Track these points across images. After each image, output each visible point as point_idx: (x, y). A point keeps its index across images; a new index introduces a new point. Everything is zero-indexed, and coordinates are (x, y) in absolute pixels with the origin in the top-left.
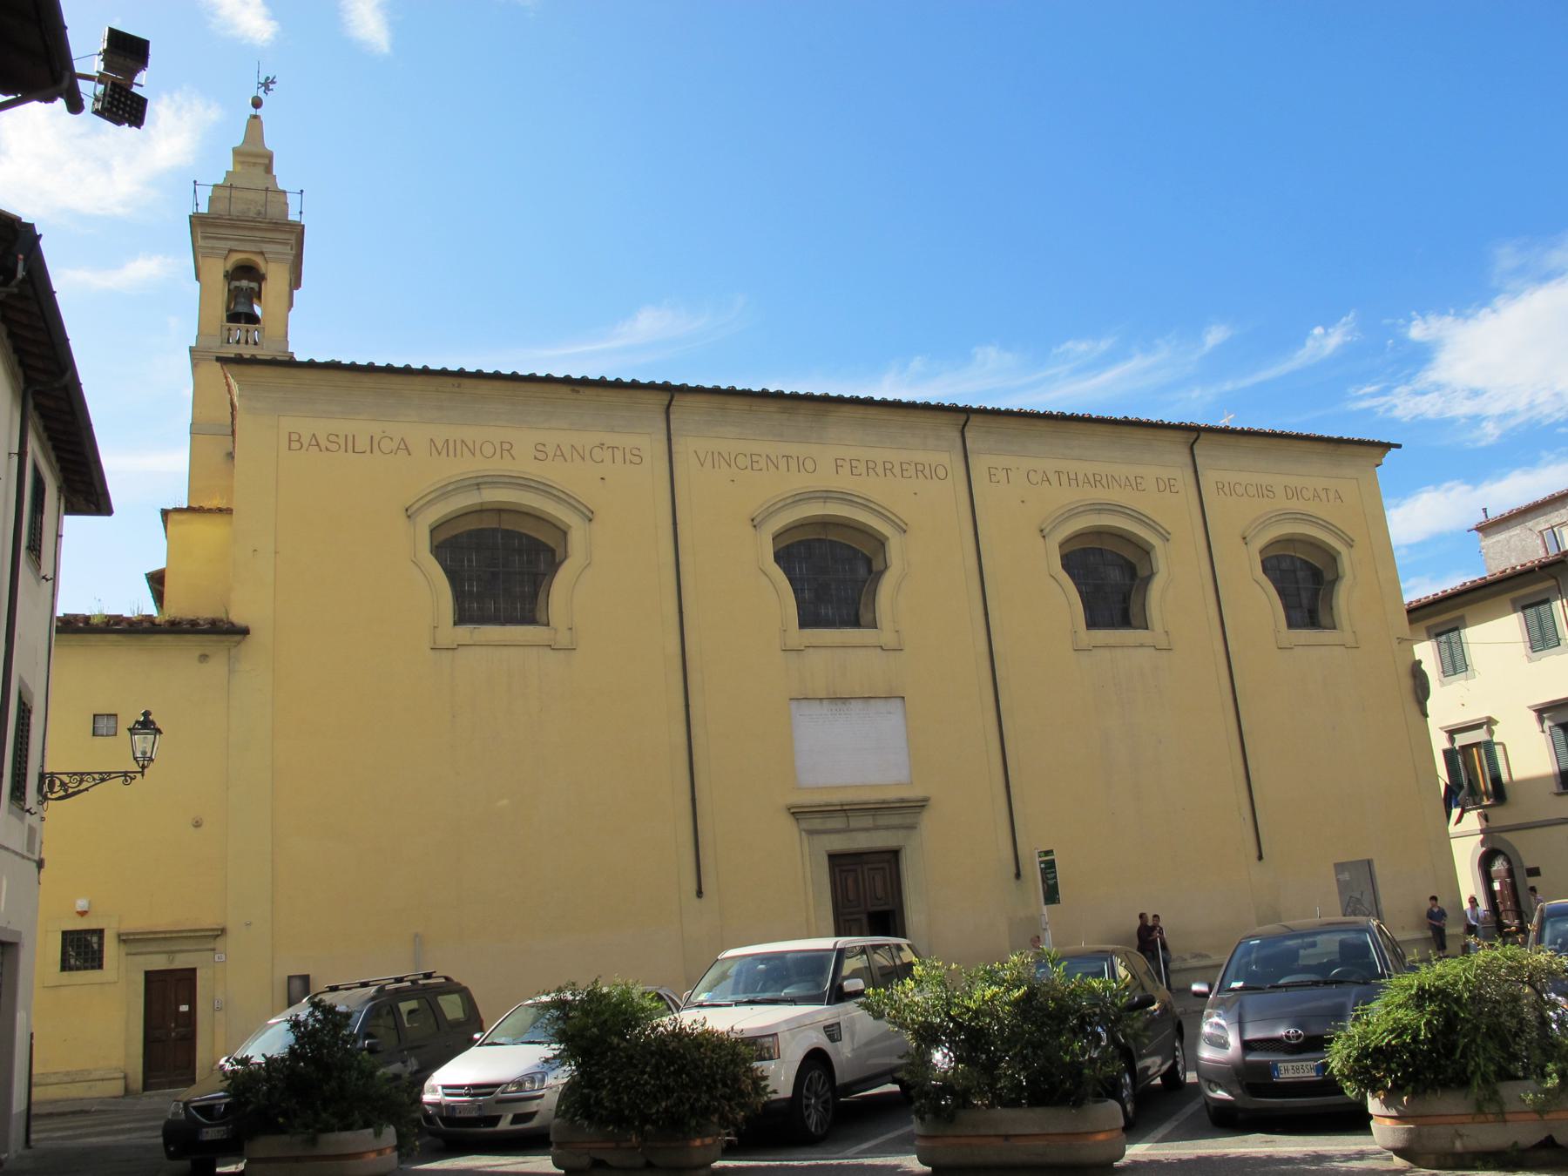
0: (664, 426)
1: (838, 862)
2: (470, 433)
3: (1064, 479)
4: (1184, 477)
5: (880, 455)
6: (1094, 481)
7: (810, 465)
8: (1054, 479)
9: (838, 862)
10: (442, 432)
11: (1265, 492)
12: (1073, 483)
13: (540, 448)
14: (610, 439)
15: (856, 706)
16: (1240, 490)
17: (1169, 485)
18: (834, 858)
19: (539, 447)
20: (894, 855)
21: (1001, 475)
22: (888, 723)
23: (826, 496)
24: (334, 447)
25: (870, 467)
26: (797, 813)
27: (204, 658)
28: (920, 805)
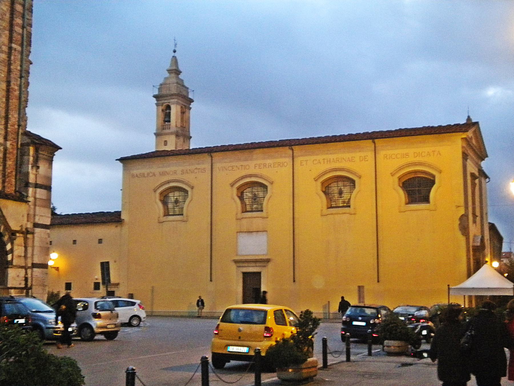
0: (210, 161)
1: (245, 275)
2: (167, 169)
3: (326, 161)
4: (370, 155)
5: (269, 161)
6: (338, 160)
7: (247, 167)
8: (322, 161)
9: (245, 275)
10: (161, 170)
11: (405, 156)
12: (329, 162)
13: (182, 171)
14: (198, 166)
15: (254, 234)
16: (399, 156)
17: (365, 159)
18: (244, 274)
19: (182, 171)
20: (259, 274)
21: (304, 163)
22: (262, 238)
23: (250, 176)
24: (140, 176)
25: (265, 165)
26: (236, 262)
27: (117, 226)
28: (268, 261)
